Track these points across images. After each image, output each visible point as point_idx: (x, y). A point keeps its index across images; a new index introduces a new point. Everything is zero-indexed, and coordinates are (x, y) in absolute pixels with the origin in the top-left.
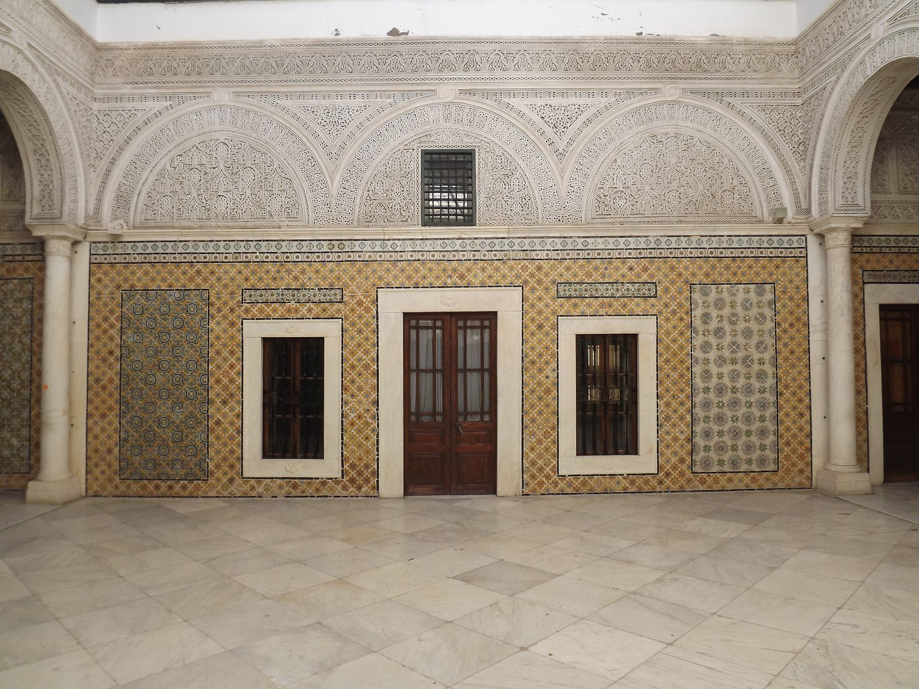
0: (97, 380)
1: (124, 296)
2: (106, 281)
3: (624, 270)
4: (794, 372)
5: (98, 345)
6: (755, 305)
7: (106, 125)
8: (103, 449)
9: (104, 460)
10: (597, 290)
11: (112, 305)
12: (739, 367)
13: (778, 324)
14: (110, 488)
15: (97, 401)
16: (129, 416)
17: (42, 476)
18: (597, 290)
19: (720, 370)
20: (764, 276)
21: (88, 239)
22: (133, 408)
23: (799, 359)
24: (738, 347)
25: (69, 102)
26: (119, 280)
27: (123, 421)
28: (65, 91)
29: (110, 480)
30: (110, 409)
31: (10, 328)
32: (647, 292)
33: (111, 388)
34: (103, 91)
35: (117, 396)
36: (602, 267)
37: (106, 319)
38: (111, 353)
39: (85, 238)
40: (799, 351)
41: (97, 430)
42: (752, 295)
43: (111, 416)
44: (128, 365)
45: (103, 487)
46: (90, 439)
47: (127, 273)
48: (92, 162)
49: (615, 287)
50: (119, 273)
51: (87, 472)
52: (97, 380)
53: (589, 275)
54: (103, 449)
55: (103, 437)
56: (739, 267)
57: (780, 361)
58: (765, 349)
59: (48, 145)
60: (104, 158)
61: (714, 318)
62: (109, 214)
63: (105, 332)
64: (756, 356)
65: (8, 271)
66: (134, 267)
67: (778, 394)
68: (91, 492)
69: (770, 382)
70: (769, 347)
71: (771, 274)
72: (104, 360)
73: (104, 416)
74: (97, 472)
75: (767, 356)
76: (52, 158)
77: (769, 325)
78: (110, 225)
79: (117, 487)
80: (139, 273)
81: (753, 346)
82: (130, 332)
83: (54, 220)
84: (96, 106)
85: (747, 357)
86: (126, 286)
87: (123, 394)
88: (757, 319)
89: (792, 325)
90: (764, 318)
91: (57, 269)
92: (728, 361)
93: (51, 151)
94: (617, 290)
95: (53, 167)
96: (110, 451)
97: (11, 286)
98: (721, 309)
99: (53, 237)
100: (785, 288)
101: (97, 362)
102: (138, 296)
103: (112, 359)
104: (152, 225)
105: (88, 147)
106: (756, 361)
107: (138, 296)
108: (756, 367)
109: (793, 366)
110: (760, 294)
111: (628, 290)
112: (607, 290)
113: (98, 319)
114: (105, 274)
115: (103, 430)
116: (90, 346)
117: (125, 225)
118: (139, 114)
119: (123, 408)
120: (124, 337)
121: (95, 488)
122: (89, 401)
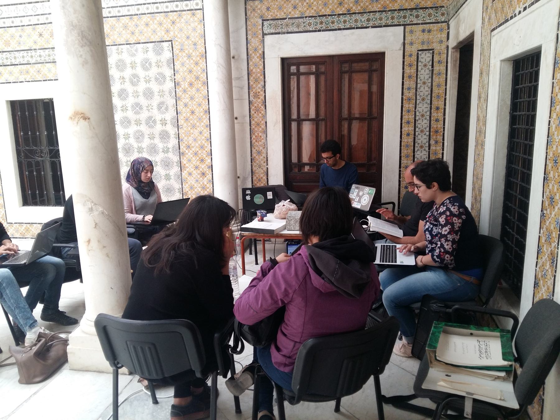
3: (35, 37)
4: (196, 132)
6: (154, 64)
10: (15, 58)
12: (143, 128)
13: (176, 84)
18: (15, 58)
19: (126, 131)
20: (161, 34)
23: (200, 119)
24: (141, 108)
32: (39, 59)
36: (17, 34)
40: (199, 111)
42: (151, 55)
49: (30, 54)
53: (7, 43)
56: (137, 26)
57: (181, 122)
58: (167, 109)
61: (117, 80)
64: (158, 117)
67: (181, 154)
69: (173, 142)
70: (170, 108)
71: (167, 31)
75: (170, 115)
77: (169, 85)
81: (155, 107)
85: (150, 118)
88: (157, 79)
89: (191, 84)
90: (164, 77)
92: (133, 122)
94: (32, 57)
98: (122, 71)
100: (182, 45)
106: (158, 122)
108: (159, 127)
109: (194, 126)
110: (158, 52)
111: (40, 56)
112: (23, 57)
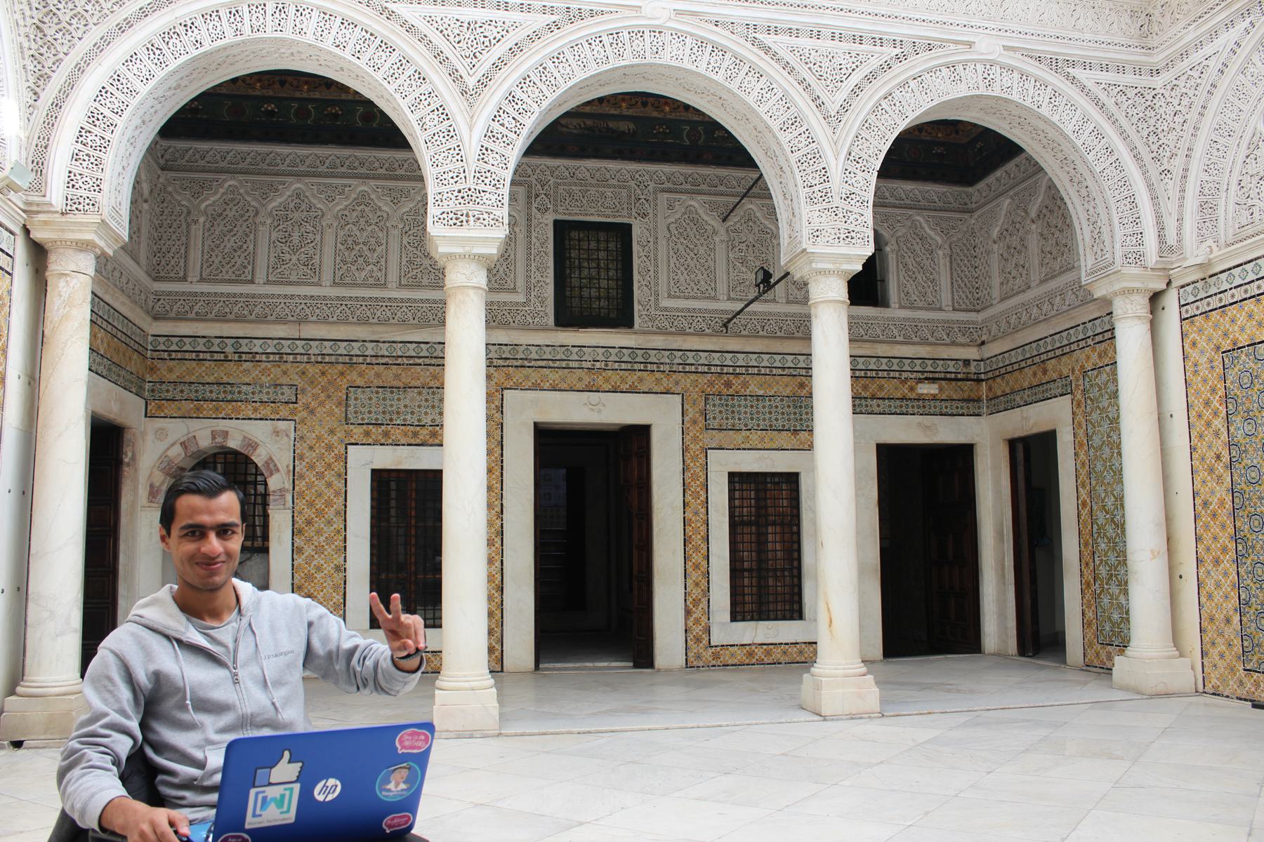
0: (1206, 504)
1: (1226, 361)
2: (1202, 344)
5: (1202, 447)
7: (1176, 102)
8: (1219, 617)
9: (1221, 634)
11: (1213, 379)
14: (1233, 685)
15: (1207, 537)
16: (1249, 562)
17: (1129, 651)
21: (1174, 284)
22: (1253, 547)
25: (1103, 96)
26: (1217, 337)
27: (1242, 571)
28: (1090, 84)
29: (1232, 670)
30: (1224, 550)
31: (1109, 436)
33: (1224, 516)
34: (1161, 56)
35: (1231, 530)
37: (1207, 403)
38: (1218, 457)
39: (1169, 284)
41: (1210, 585)
43: (1227, 563)
44: (1242, 475)
45: (1224, 681)
46: (1203, 600)
47: (1225, 323)
48: (1166, 166)
50: (1216, 326)
51: (1204, 654)
52: (1206, 504)
54: (1219, 617)
55: (1218, 596)
59: (1081, 168)
60: (1179, 152)
62: (1195, 236)
63: (1208, 424)
65: (1100, 356)
66: (1232, 311)
68: (1209, 688)
72: (1211, 470)
73: (1217, 562)
74: (1214, 653)
76: (1090, 182)
78: (1195, 253)
79: (1241, 683)
80: (1241, 319)
82: (1238, 419)
83: (1104, 270)
84: (1158, 82)
86: (1226, 345)
87: (1238, 524)
91: (1131, 339)
93: (1086, 174)
95: (1094, 194)
96: (1228, 621)
97: (1104, 376)
99: (1115, 294)
101: (1203, 474)
102: (1243, 357)
103: (1220, 468)
104: (1250, 232)
105: (1154, 147)
107: (1243, 357)
113: (1198, 405)
114: (1200, 331)
115: (1218, 585)
116: (1193, 449)
117: (1214, 246)
118: (1211, 63)
119: (1240, 548)
120: (1232, 429)
121: (1214, 681)
122: (1198, 539)
